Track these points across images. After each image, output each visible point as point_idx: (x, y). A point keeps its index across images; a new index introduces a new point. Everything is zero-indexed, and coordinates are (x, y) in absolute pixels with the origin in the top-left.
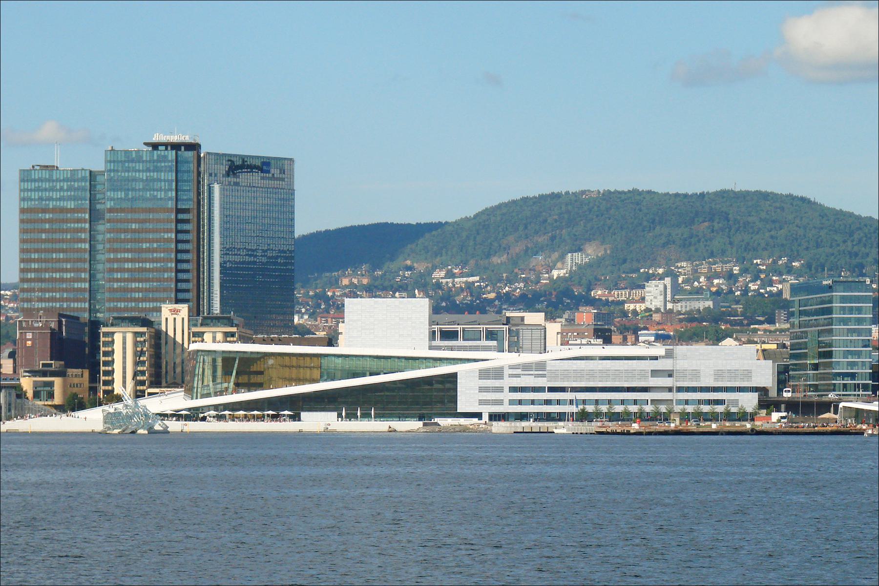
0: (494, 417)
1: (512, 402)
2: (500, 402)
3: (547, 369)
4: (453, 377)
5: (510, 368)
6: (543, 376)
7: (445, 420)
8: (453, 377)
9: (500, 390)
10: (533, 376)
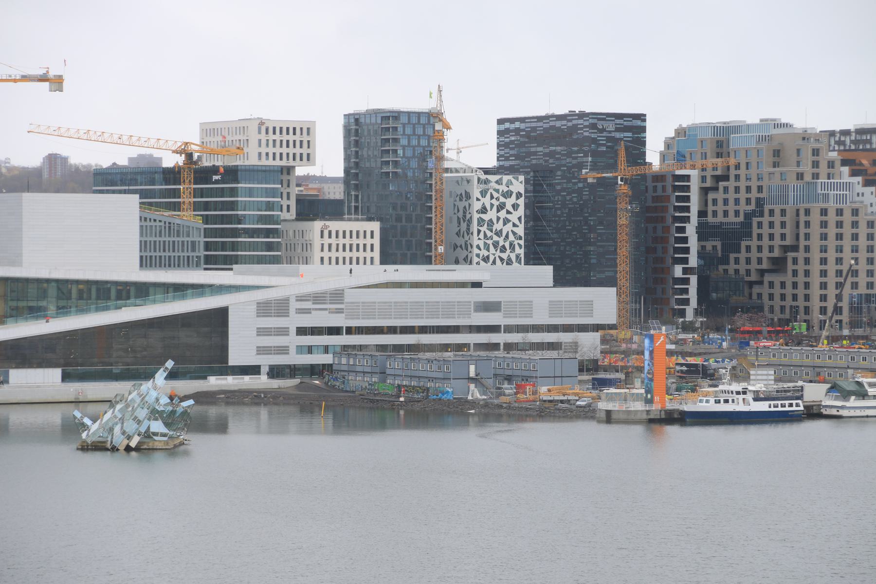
0: (275, 372)
1: (300, 349)
2: (283, 350)
3: (346, 300)
4: (222, 314)
5: (297, 300)
6: (339, 311)
7: (224, 379)
8: (222, 314)
9: (283, 332)
10: (327, 312)
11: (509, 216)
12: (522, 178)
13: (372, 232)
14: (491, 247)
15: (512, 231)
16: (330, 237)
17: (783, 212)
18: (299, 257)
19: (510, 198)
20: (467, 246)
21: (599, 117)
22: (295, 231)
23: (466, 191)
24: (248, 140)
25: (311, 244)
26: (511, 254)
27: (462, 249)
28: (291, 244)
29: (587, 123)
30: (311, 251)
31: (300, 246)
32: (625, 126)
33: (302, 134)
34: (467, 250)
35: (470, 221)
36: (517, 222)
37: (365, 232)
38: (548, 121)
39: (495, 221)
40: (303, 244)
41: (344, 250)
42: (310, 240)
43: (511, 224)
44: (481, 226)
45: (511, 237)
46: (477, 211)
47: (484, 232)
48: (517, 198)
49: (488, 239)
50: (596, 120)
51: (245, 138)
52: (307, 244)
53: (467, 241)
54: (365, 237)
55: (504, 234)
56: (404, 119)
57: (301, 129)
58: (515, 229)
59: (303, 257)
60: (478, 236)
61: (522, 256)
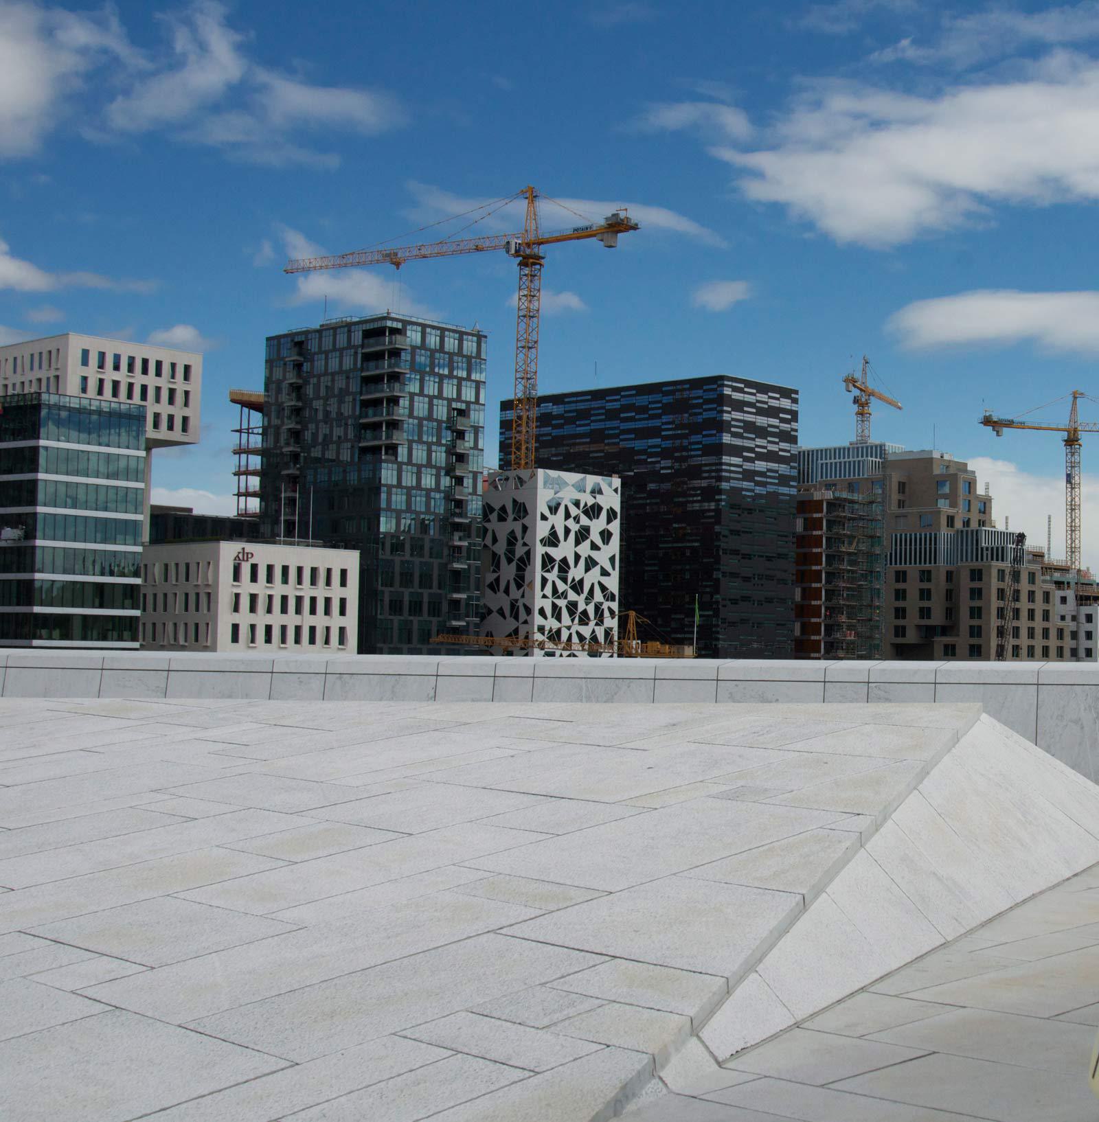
11: (595, 554)
12: (617, 482)
13: (344, 573)
14: (565, 613)
15: (599, 583)
16: (254, 578)
17: (926, 576)
18: (175, 624)
19: (598, 518)
20: (520, 611)
21: (734, 384)
22: (166, 566)
23: (515, 501)
24: (57, 377)
25: (209, 594)
26: (597, 628)
27: (505, 618)
28: (155, 595)
29: (712, 395)
30: (209, 610)
31: (180, 599)
32: (770, 407)
33: (173, 377)
34: (516, 618)
35: (526, 560)
36: (608, 567)
37: (329, 571)
38: (618, 397)
39: (571, 561)
40: (187, 595)
41: (284, 610)
42: (208, 585)
43: (597, 570)
44: (548, 571)
45: (598, 596)
46: (541, 541)
47: (554, 582)
48: (609, 521)
49: (559, 597)
50: (730, 390)
51: (52, 373)
52: (198, 594)
53: (517, 601)
54: (328, 583)
55: (586, 588)
56: (414, 336)
57: (173, 366)
58: (604, 580)
59: (186, 624)
60: (542, 590)
61: (615, 632)
